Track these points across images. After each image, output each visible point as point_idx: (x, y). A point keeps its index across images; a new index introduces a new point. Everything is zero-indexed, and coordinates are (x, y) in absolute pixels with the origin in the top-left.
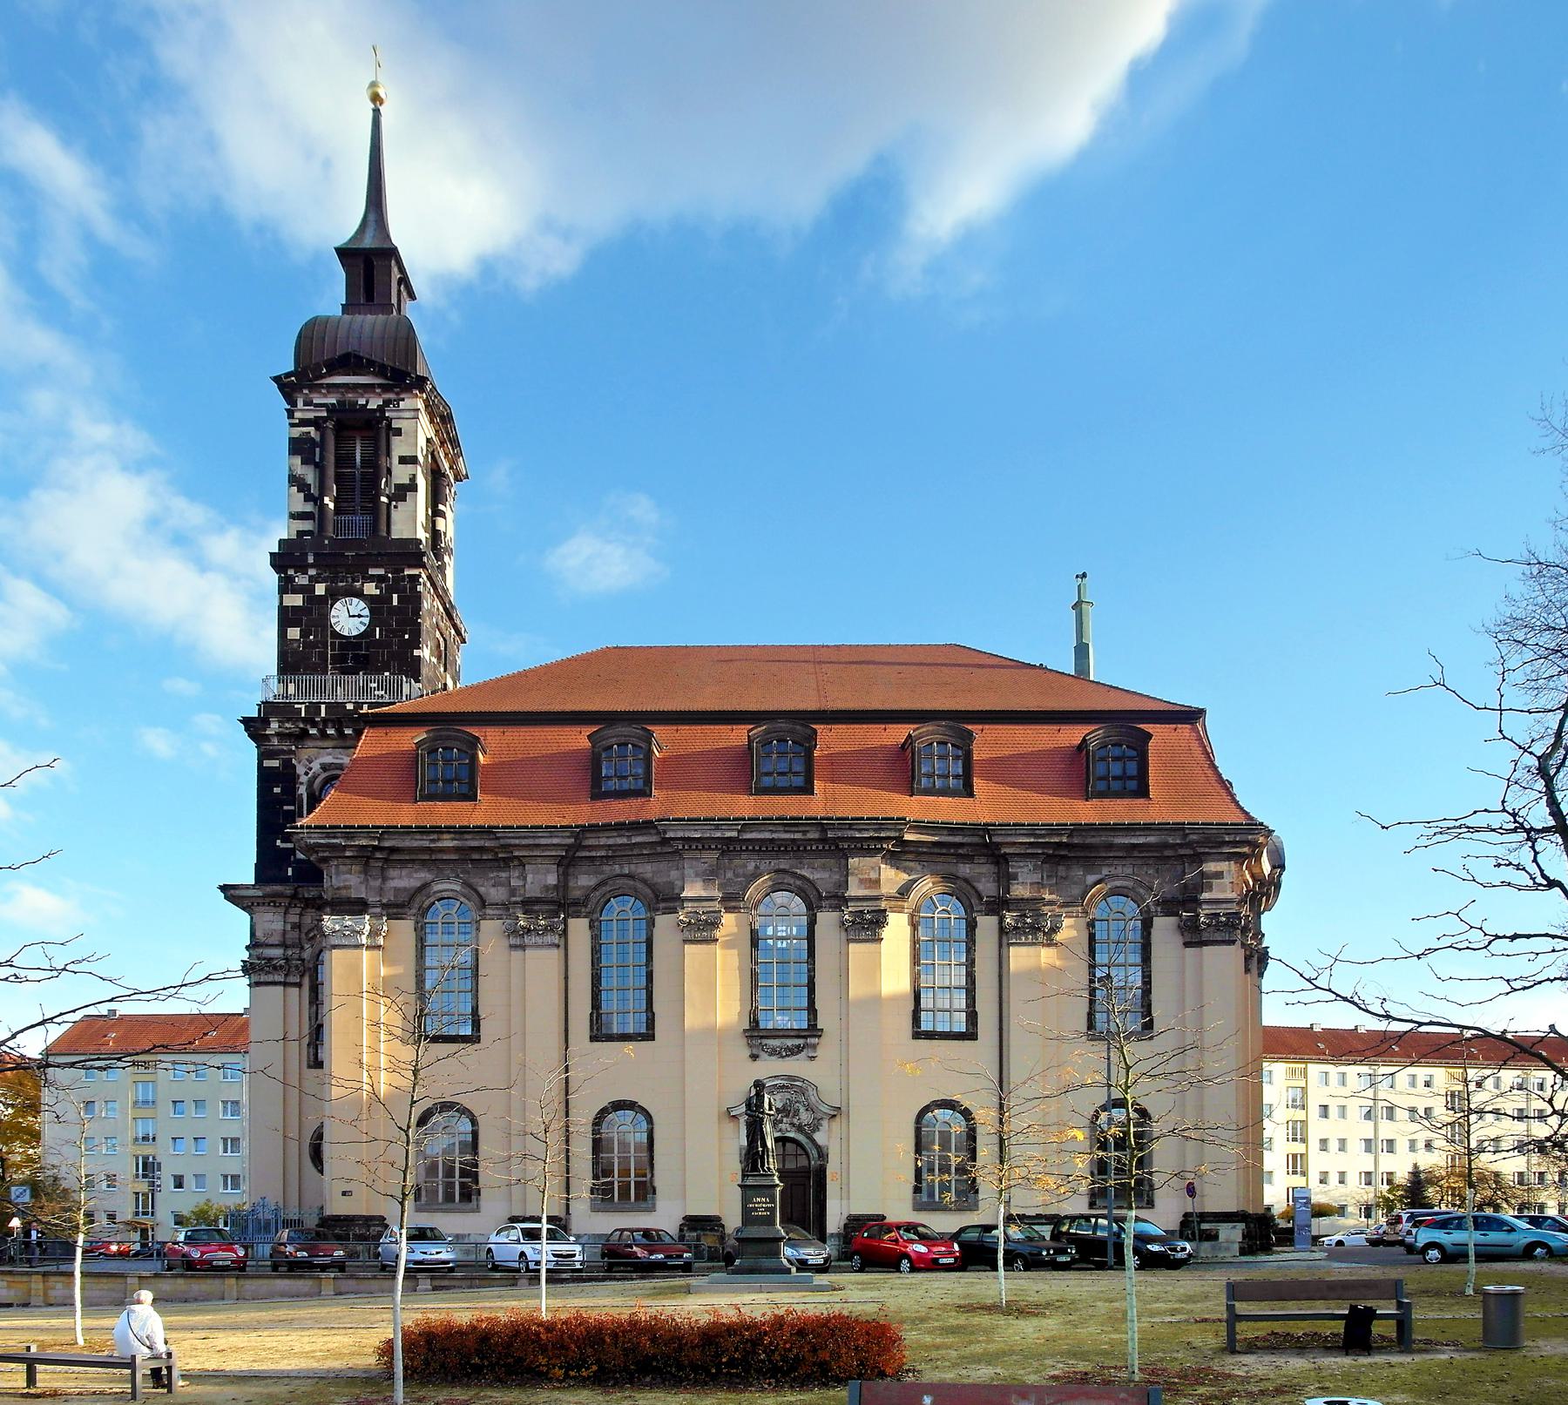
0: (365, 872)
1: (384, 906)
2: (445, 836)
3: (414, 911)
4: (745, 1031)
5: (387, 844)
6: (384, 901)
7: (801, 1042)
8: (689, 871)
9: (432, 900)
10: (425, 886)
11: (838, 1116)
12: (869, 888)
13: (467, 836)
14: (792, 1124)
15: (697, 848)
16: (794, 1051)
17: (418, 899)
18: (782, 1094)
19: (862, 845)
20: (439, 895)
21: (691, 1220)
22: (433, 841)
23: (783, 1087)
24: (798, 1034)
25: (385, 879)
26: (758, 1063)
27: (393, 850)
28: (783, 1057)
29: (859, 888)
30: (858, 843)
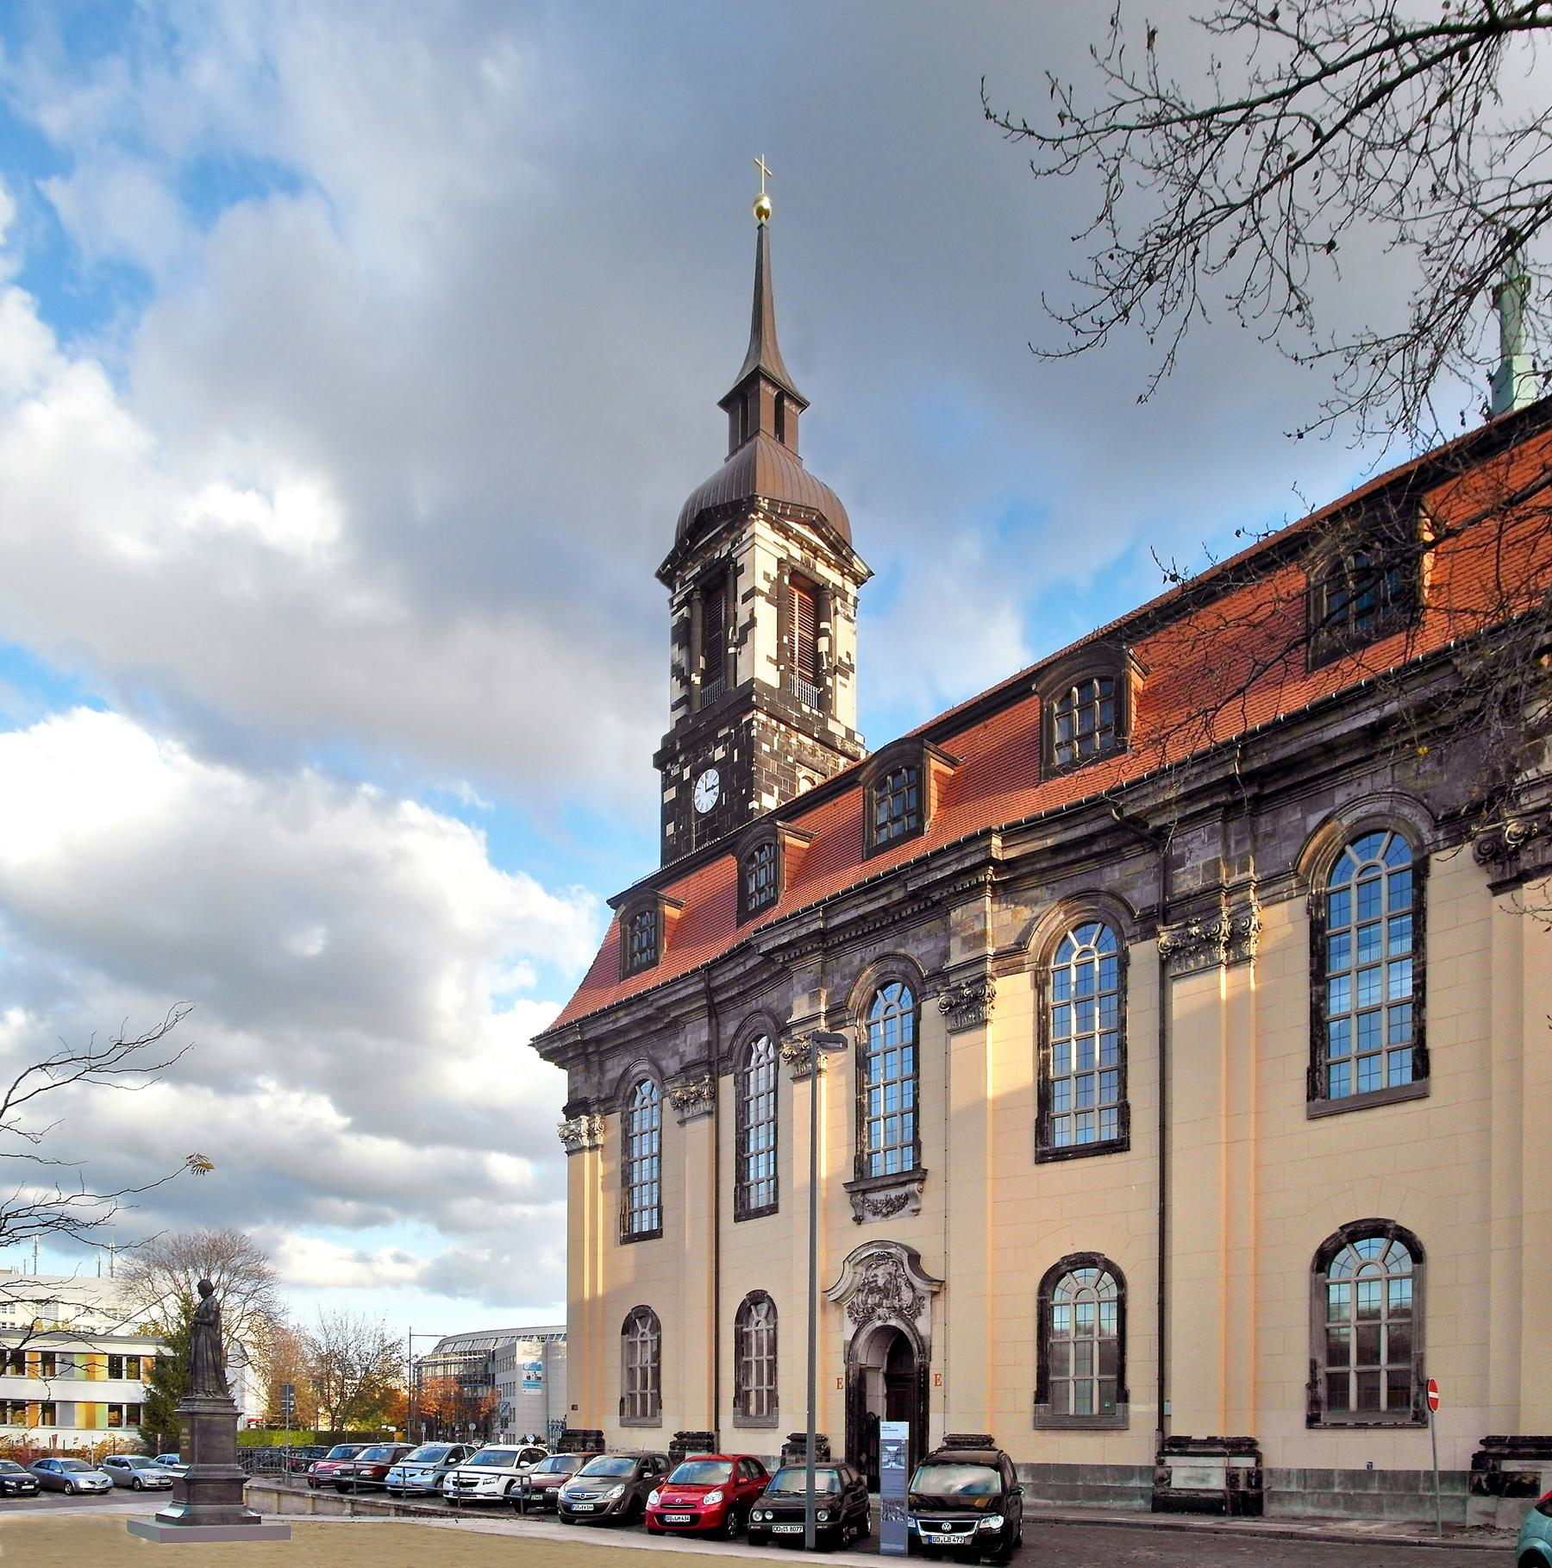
0: (587, 1069)
1: (599, 1101)
2: (621, 1014)
3: (620, 1101)
4: (846, 1185)
5: (587, 1036)
6: (603, 1096)
7: (901, 1191)
8: (798, 988)
9: (632, 1085)
10: (626, 1071)
11: (942, 1295)
12: (973, 948)
13: (634, 1009)
14: (893, 1309)
15: (797, 958)
16: (895, 1206)
17: (622, 1088)
18: (883, 1267)
19: (955, 888)
20: (636, 1079)
21: (797, 1440)
22: (614, 1022)
23: (881, 1257)
24: (901, 1179)
25: (602, 1071)
26: (864, 1226)
27: (598, 1040)
28: (887, 1215)
29: (963, 952)
30: (949, 886)
